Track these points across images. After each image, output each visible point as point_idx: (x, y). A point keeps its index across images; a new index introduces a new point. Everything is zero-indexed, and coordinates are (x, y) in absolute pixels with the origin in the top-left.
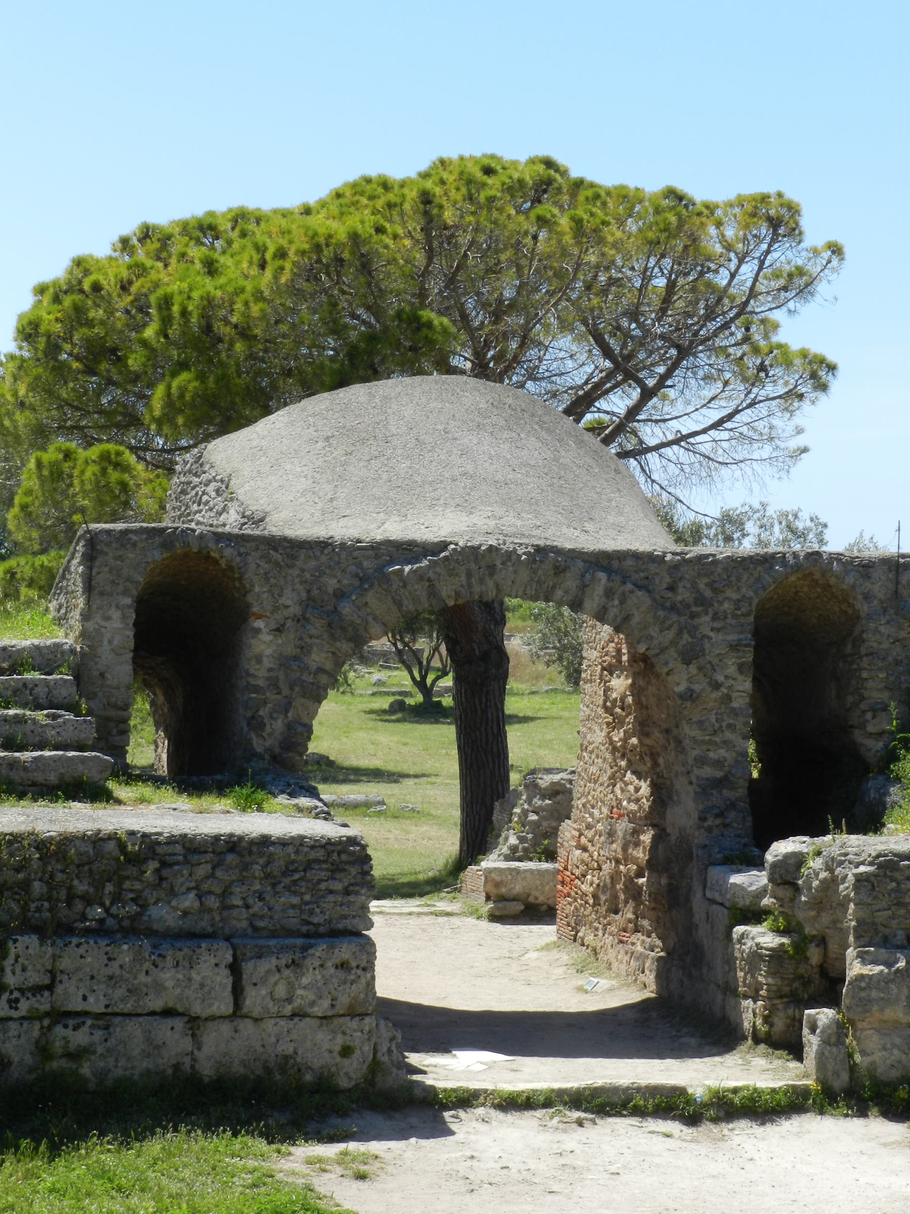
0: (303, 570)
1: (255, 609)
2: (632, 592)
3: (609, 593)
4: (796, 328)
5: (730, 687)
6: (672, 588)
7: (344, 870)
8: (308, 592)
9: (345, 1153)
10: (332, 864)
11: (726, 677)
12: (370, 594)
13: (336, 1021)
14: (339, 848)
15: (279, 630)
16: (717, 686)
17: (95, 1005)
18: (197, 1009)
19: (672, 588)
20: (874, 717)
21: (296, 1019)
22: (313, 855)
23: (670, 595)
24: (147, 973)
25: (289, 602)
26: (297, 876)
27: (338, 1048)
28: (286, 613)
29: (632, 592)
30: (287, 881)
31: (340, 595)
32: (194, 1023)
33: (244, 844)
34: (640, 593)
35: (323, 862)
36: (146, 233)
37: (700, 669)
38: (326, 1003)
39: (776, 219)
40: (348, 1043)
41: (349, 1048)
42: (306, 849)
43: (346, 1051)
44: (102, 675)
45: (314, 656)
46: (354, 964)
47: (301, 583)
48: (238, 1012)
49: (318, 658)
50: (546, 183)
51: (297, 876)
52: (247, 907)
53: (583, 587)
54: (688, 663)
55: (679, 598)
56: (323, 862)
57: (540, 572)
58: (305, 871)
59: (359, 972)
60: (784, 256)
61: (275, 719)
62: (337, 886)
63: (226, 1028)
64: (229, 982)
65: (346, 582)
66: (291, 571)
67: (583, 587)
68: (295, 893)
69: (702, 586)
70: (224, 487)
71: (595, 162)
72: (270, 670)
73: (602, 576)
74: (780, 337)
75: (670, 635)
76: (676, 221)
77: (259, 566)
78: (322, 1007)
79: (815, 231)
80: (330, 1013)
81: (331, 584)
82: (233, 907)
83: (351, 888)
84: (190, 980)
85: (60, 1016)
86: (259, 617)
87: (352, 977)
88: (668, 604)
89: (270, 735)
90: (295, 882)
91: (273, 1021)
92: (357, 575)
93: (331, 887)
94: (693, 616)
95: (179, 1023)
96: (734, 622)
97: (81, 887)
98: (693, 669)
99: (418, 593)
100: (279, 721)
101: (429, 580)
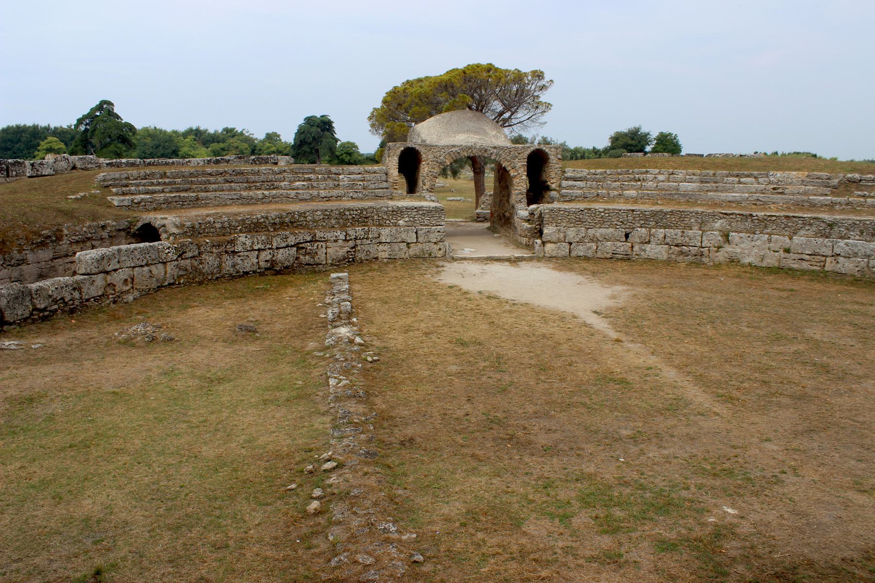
4: (544, 97)
9: (119, 251)
17: (388, 241)
32: (408, 244)
36: (408, 82)
39: (538, 75)
43: (440, 249)
50: (490, 68)
60: (541, 83)
70: (419, 135)
71: (502, 64)
74: (540, 100)
76: (519, 77)
78: (435, 240)
79: (547, 78)
85: (380, 243)
97: (385, 217)
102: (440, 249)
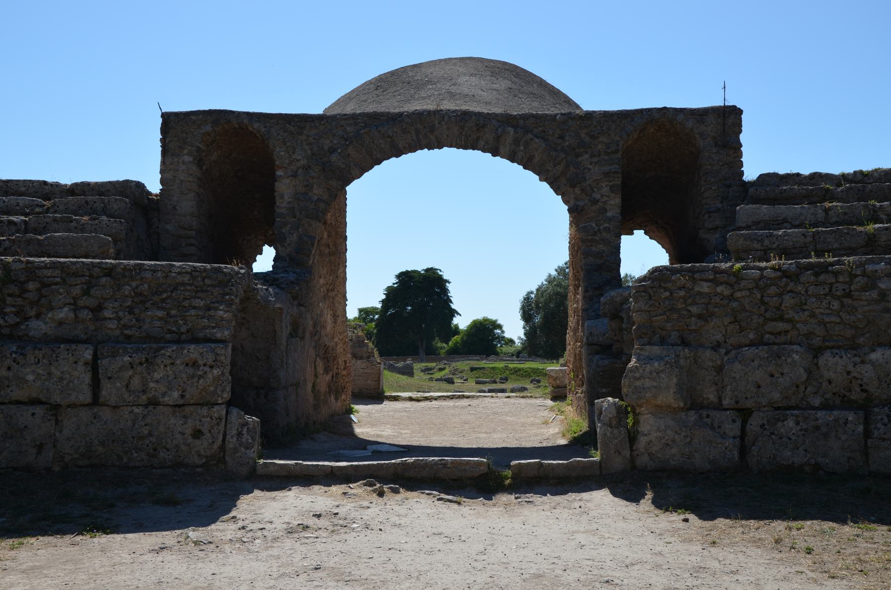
0: (308, 136)
1: (277, 163)
2: (532, 140)
3: (516, 142)
5: (605, 203)
6: (561, 137)
7: (208, 291)
8: (311, 150)
10: (196, 287)
11: (602, 196)
12: (350, 148)
13: (188, 410)
14: (204, 274)
15: (294, 176)
16: (595, 202)
18: (57, 398)
19: (561, 137)
20: (710, 217)
21: (151, 408)
22: (180, 279)
23: (560, 141)
24: (9, 368)
25: (299, 157)
26: (165, 295)
27: (189, 432)
28: (299, 164)
29: (532, 140)
30: (156, 298)
31: (332, 150)
32: (55, 409)
33: (119, 270)
34: (537, 140)
35: (188, 284)
37: (583, 190)
38: (176, 394)
40: (198, 427)
41: (199, 431)
42: (174, 275)
43: (197, 434)
44: (174, 208)
45: (315, 191)
46: (201, 362)
47: (307, 144)
48: (96, 401)
49: (317, 192)
51: (165, 295)
52: (119, 319)
53: (498, 138)
54: (573, 186)
55: (567, 143)
56: (188, 284)
57: (466, 129)
58: (172, 292)
59: (207, 369)
61: (292, 234)
62: (198, 302)
63: (85, 415)
64: (87, 378)
65: (335, 141)
66: (300, 137)
67: (498, 138)
68: (163, 309)
69: (583, 135)
72: (289, 203)
73: (511, 130)
75: (560, 168)
77: (279, 134)
80: (181, 402)
81: (327, 144)
82: (106, 319)
83: (212, 305)
84: (49, 374)
86: (281, 168)
87: (200, 373)
88: (559, 148)
89: (289, 245)
90: (163, 300)
91: (130, 409)
92: (343, 137)
93: (194, 304)
94: (577, 156)
95: (39, 410)
96: (606, 158)
98: (577, 191)
99: (383, 146)
100: (295, 235)
101: (388, 136)
102: (197, 434)
